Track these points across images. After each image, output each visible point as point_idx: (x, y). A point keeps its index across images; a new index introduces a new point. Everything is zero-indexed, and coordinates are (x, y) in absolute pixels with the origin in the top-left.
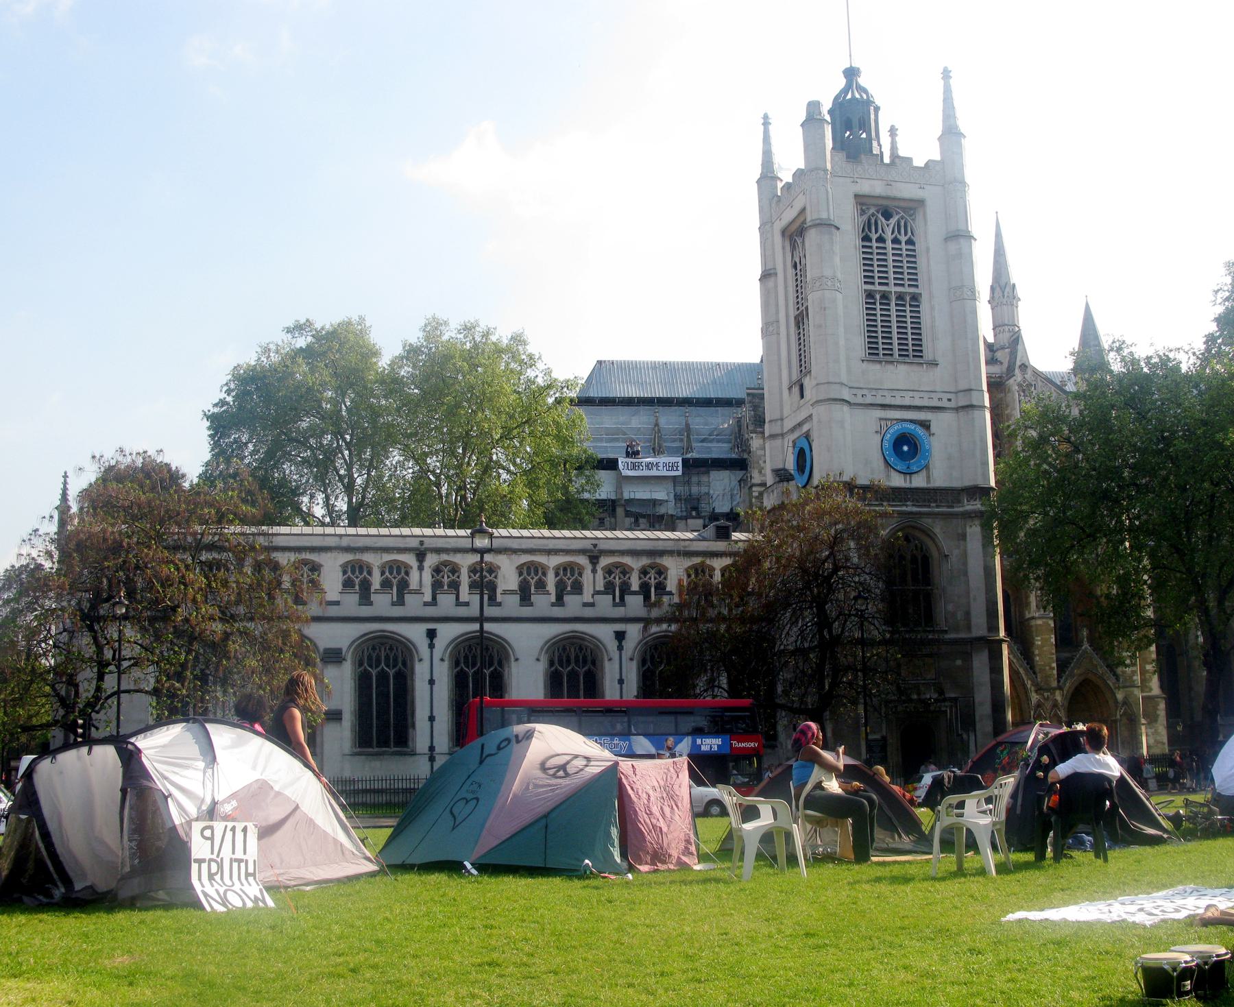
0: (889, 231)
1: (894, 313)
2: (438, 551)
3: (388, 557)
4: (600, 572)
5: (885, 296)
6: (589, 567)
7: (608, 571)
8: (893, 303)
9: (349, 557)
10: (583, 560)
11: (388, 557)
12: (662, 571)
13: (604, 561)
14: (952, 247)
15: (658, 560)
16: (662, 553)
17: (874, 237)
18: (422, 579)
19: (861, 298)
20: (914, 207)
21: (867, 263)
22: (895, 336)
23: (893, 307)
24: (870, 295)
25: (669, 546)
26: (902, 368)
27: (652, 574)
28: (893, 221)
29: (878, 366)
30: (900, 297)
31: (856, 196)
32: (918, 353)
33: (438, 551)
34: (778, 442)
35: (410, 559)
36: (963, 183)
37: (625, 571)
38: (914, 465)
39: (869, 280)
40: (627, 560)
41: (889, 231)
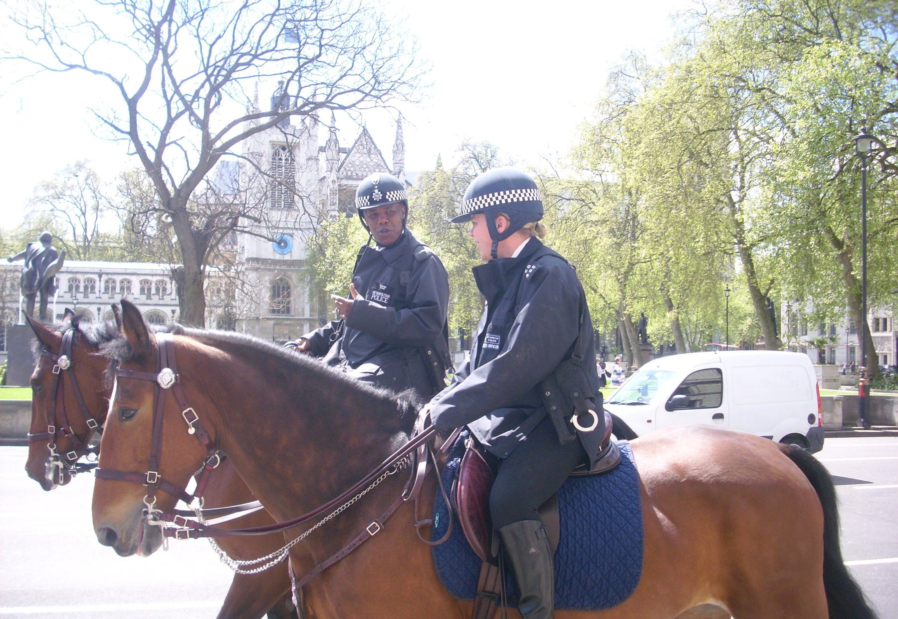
2: (107, 274)
18: (100, 285)
35: (96, 277)
38: (288, 250)
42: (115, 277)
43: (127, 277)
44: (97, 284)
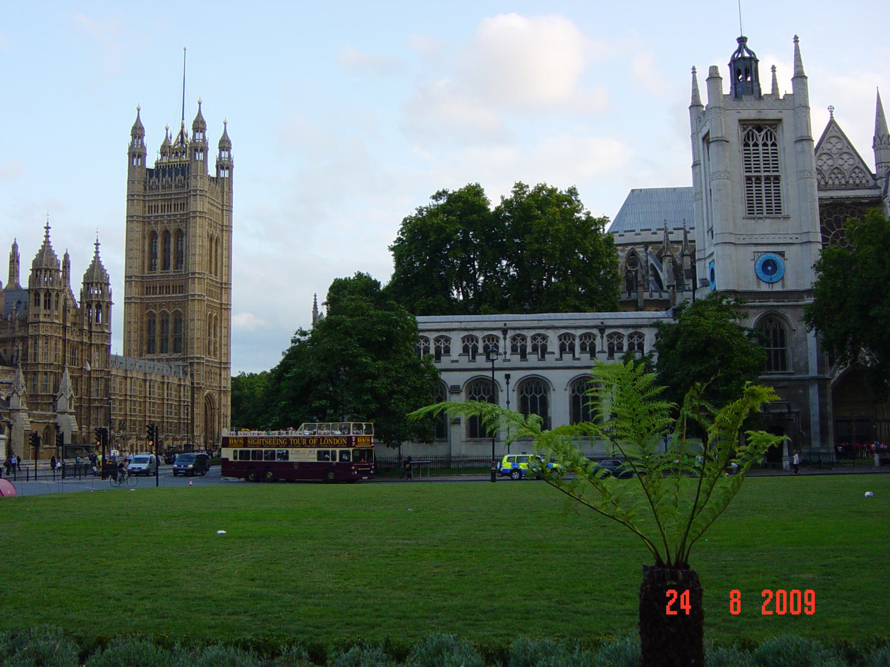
0: (760, 139)
1: (763, 188)
2: (514, 329)
3: (486, 333)
4: (605, 338)
5: (758, 178)
6: (599, 335)
7: (610, 336)
8: (763, 183)
9: (466, 333)
10: (595, 331)
11: (486, 333)
12: (641, 336)
13: (608, 332)
14: (799, 146)
15: (639, 330)
16: (641, 326)
17: (751, 143)
18: (505, 344)
19: (743, 181)
20: (776, 123)
21: (747, 159)
22: (764, 202)
23: (763, 184)
24: (749, 178)
25: (645, 322)
26: (768, 221)
27: (636, 337)
28: (763, 133)
29: (753, 221)
30: (767, 178)
31: (740, 120)
32: (779, 210)
33: (514, 329)
34: (702, 263)
35: (499, 334)
36: (807, 108)
37: (620, 336)
39: (748, 169)
40: (621, 331)
41: (760, 139)
42: (524, 332)
43: (542, 332)
44: (501, 343)
